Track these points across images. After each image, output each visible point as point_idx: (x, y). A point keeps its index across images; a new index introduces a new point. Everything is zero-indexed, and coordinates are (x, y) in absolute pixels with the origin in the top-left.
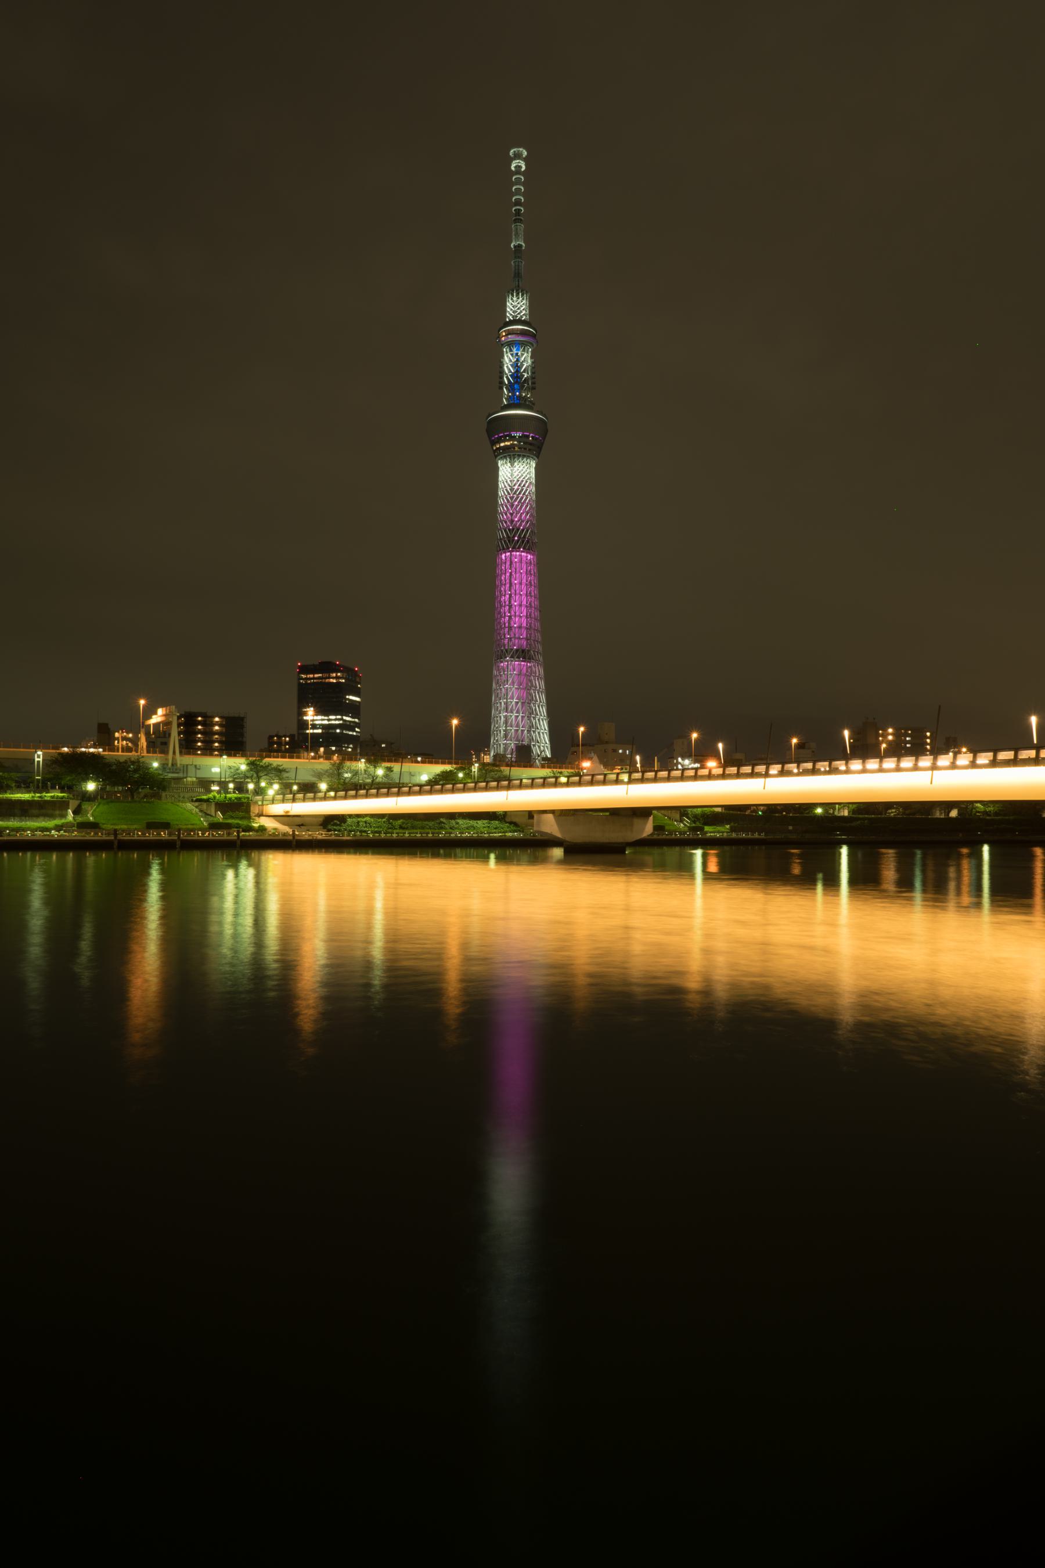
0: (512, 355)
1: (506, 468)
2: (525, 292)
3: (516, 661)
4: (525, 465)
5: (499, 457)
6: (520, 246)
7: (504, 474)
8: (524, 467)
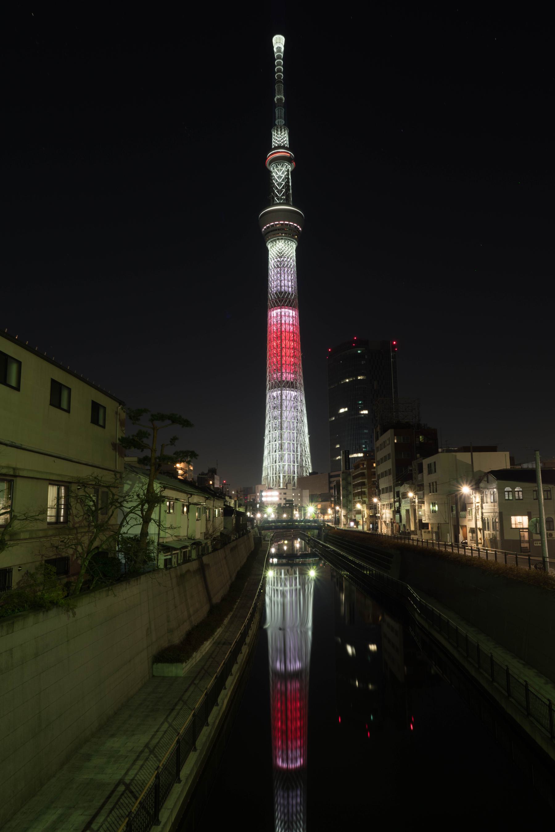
0: (278, 170)
1: (275, 248)
2: (286, 129)
3: (288, 390)
4: (289, 246)
5: (269, 241)
6: (281, 99)
7: (273, 252)
8: (289, 248)
